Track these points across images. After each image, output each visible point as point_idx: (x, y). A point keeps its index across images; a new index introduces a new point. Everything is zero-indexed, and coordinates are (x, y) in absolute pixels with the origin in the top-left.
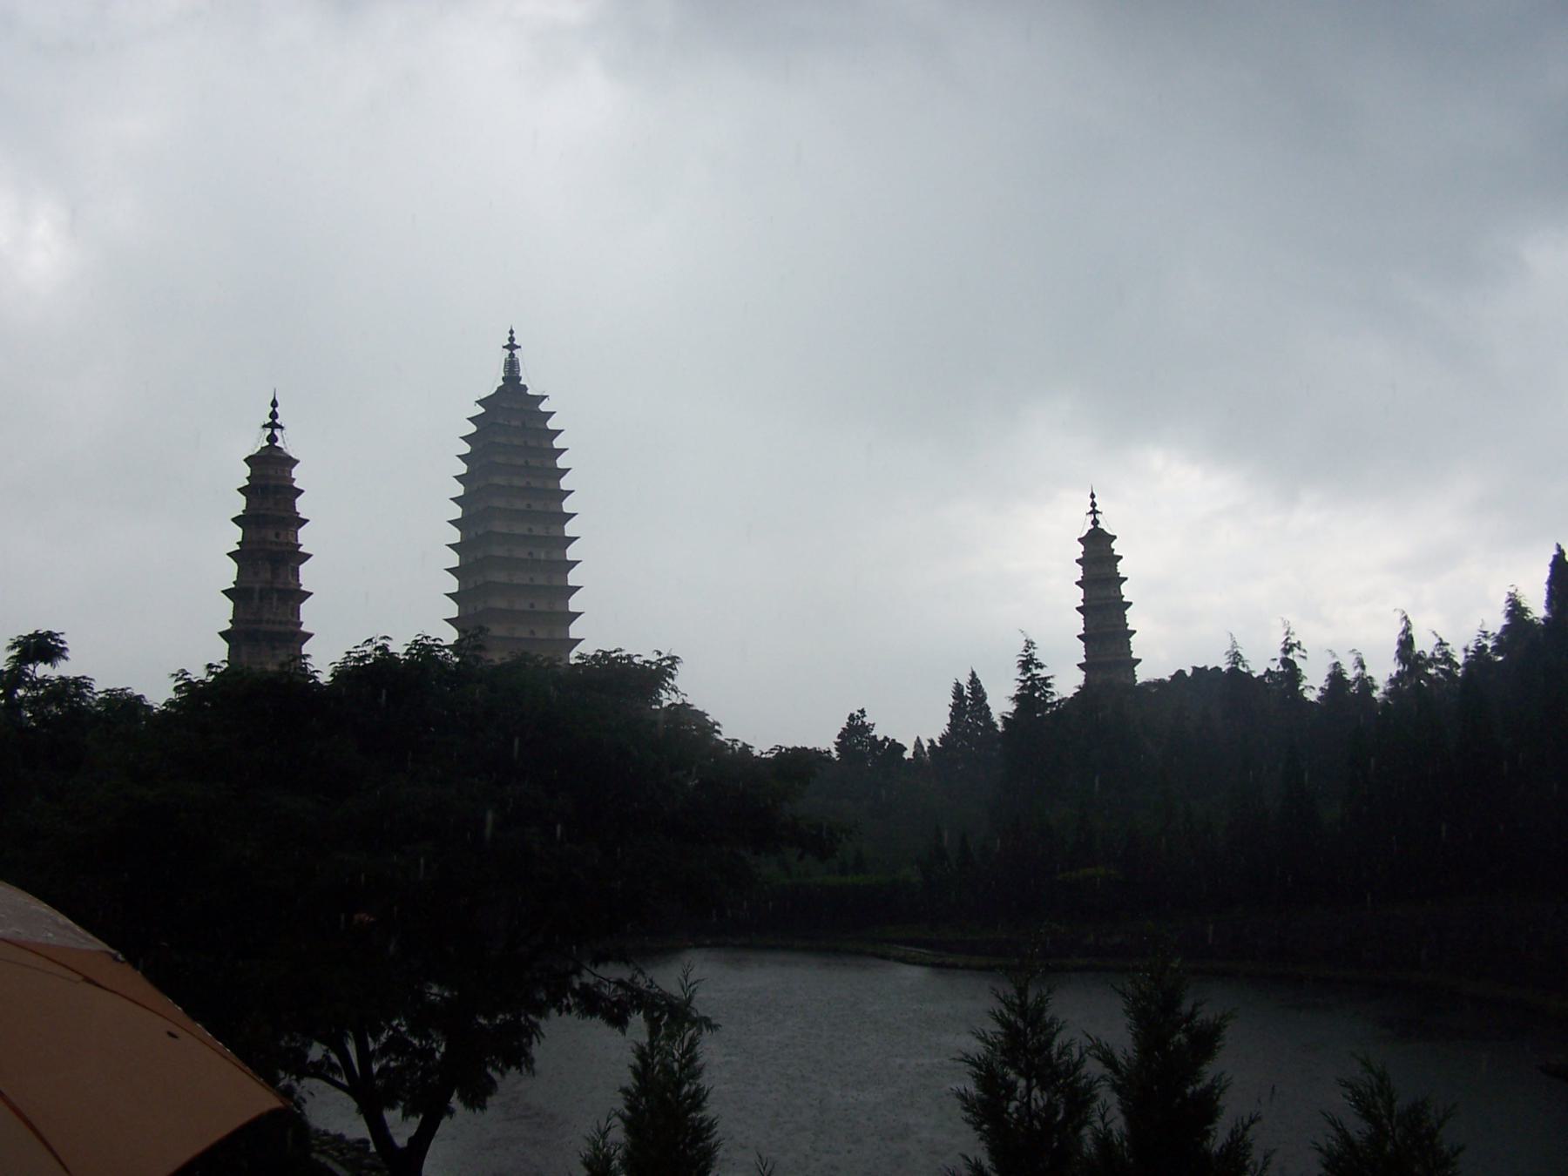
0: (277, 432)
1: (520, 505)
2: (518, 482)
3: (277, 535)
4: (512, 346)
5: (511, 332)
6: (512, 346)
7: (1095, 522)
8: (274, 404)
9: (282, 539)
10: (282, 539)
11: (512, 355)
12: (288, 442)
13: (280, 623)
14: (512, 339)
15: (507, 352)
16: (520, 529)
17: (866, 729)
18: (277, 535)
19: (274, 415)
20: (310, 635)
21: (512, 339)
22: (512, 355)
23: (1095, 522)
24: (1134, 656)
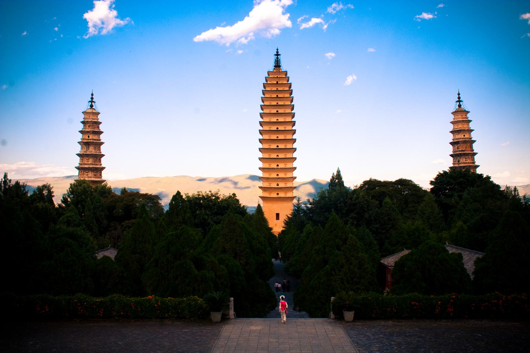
0: (93, 103)
1: (274, 111)
2: (274, 103)
3: (89, 137)
4: (277, 55)
5: (277, 50)
6: (277, 55)
7: (460, 106)
8: (92, 95)
9: (90, 138)
10: (90, 138)
11: (277, 58)
12: (98, 107)
14: (277, 52)
16: (274, 119)
18: (89, 137)
19: (92, 98)
20: (105, 168)
21: (277, 52)
22: (277, 58)
23: (460, 106)
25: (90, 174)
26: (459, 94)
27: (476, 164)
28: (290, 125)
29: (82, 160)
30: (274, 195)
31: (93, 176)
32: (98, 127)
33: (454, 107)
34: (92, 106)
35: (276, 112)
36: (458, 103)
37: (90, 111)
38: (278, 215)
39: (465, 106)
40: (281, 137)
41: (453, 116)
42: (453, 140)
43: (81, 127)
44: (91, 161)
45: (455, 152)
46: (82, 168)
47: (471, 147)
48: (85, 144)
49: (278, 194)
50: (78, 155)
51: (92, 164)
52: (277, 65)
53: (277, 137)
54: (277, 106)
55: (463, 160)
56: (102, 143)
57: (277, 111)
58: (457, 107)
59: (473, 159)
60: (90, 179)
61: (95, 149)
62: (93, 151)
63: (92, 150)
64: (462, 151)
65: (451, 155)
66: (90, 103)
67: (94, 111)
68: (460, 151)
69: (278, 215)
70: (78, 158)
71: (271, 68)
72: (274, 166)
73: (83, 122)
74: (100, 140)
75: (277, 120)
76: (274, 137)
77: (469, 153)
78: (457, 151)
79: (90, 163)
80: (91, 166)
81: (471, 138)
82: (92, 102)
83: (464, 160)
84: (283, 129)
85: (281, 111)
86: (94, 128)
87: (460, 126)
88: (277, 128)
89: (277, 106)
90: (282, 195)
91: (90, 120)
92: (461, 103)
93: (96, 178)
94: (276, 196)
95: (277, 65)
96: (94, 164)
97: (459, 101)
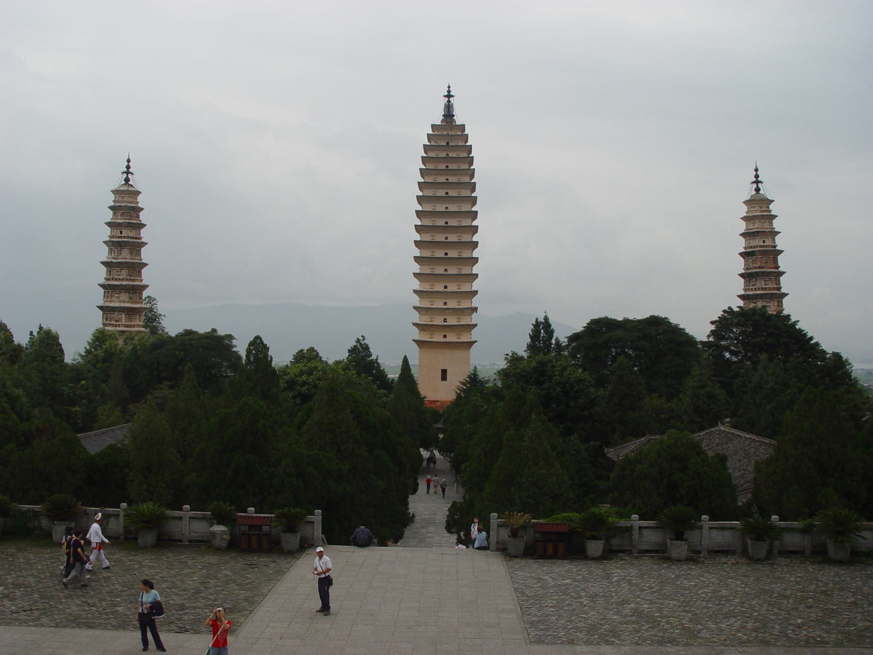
0: (130, 176)
1: (441, 193)
3: (121, 233)
4: (449, 96)
5: (449, 87)
6: (449, 96)
7: (758, 190)
8: (129, 161)
9: (123, 235)
10: (123, 235)
11: (449, 101)
14: (449, 92)
17: (366, 348)
18: (121, 233)
19: (128, 167)
20: (148, 286)
21: (449, 92)
22: (449, 101)
23: (758, 190)
24: (783, 290)
25: (124, 296)
26: (756, 170)
27: (783, 290)
28: (467, 175)
29: (109, 272)
30: (438, 338)
31: (127, 299)
32: (138, 217)
33: (748, 192)
34: (127, 180)
35: (444, 195)
36: (755, 186)
37: (125, 188)
38: (444, 373)
39: (767, 191)
40: (453, 208)
41: (745, 208)
42: (745, 248)
43: (109, 215)
44: (124, 273)
45: (748, 269)
46: (109, 285)
47: (775, 261)
48: (114, 245)
49: (445, 336)
50: (103, 263)
51: (127, 280)
53: (447, 208)
54: (447, 184)
55: (760, 283)
56: (144, 244)
57: (447, 193)
59: (778, 283)
60: (123, 305)
61: (131, 254)
62: (129, 256)
63: (125, 256)
64: (759, 268)
65: (741, 275)
66: (125, 175)
67: (130, 189)
68: (755, 268)
69: (444, 373)
70: (104, 269)
71: (438, 120)
72: (439, 287)
73: (111, 208)
74: (140, 238)
75: (447, 208)
76: (440, 238)
77: (770, 273)
78: (751, 269)
79: (123, 278)
80: (124, 283)
81: (775, 247)
82: (128, 173)
83: (763, 283)
84: (456, 168)
85: (453, 193)
86: (131, 218)
87: (756, 226)
88: (447, 193)
89: (447, 184)
90: (452, 338)
91: (123, 204)
92: (760, 185)
93: (132, 303)
94: (442, 340)
96: (130, 280)
97: (757, 182)
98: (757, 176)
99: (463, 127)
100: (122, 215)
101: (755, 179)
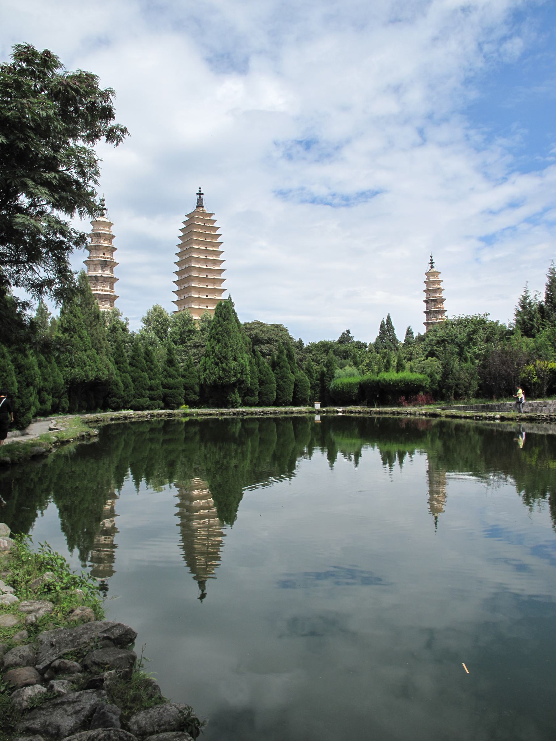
4: (200, 194)
6: (200, 194)
7: (432, 267)
11: (200, 197)
13: (105, 291)
15: (198, 196)
22: (200, 197)
23: (432, 267)
52: (200, 204)
58: (430, 268)
65: (425, 312)
95: (200, 204)
98: (432, 260)
99: (212, 214)
100: (104, 241)
101: (430, 261)
